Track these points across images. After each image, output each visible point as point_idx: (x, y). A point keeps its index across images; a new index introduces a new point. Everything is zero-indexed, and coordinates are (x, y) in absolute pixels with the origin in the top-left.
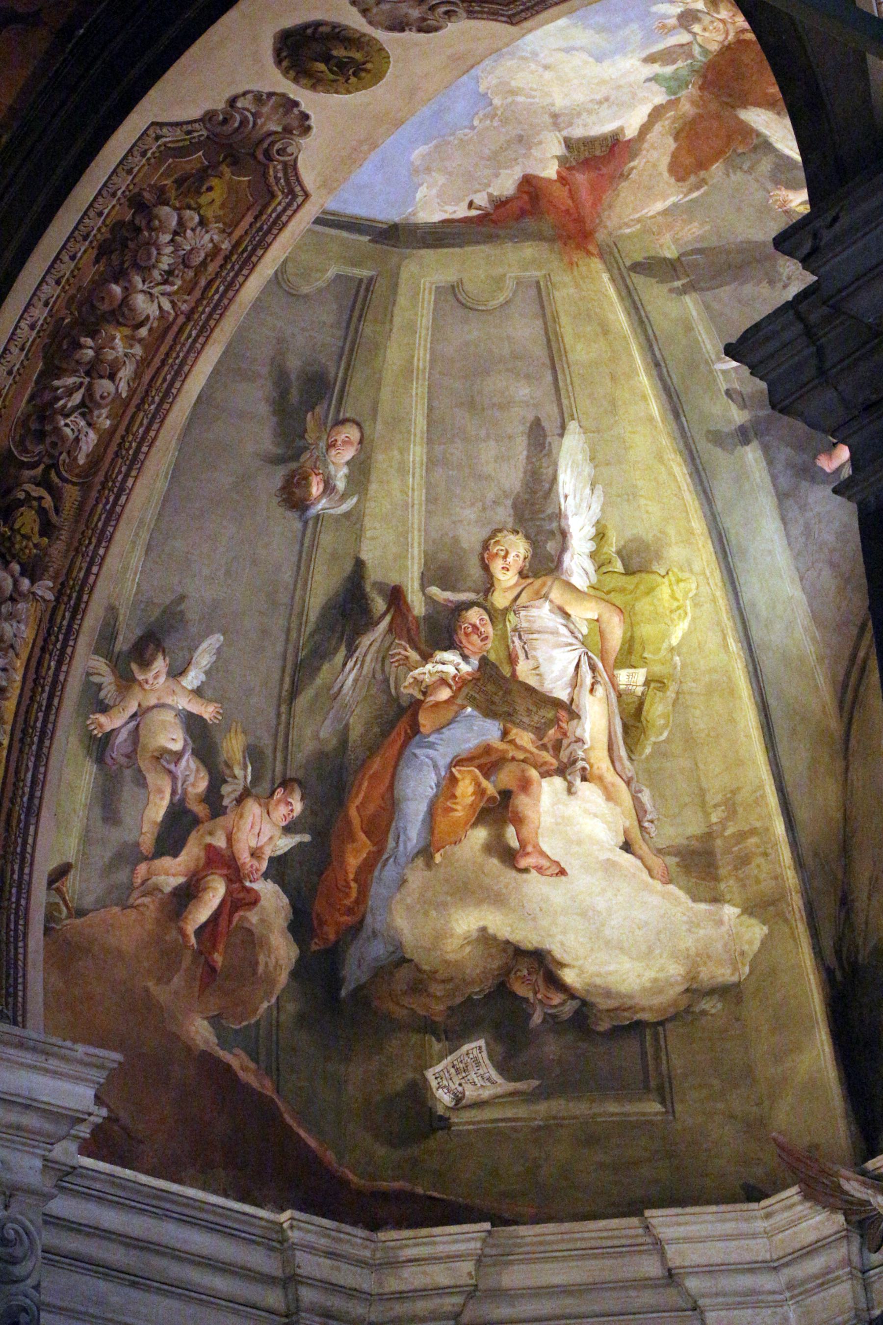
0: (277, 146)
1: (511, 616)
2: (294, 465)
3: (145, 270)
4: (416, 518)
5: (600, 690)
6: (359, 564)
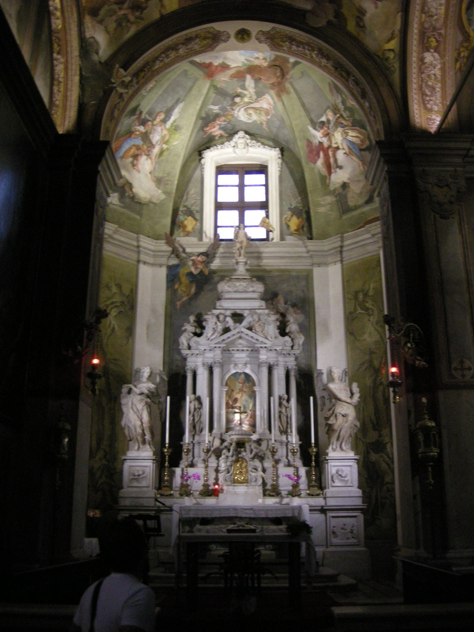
6: (139, 105)
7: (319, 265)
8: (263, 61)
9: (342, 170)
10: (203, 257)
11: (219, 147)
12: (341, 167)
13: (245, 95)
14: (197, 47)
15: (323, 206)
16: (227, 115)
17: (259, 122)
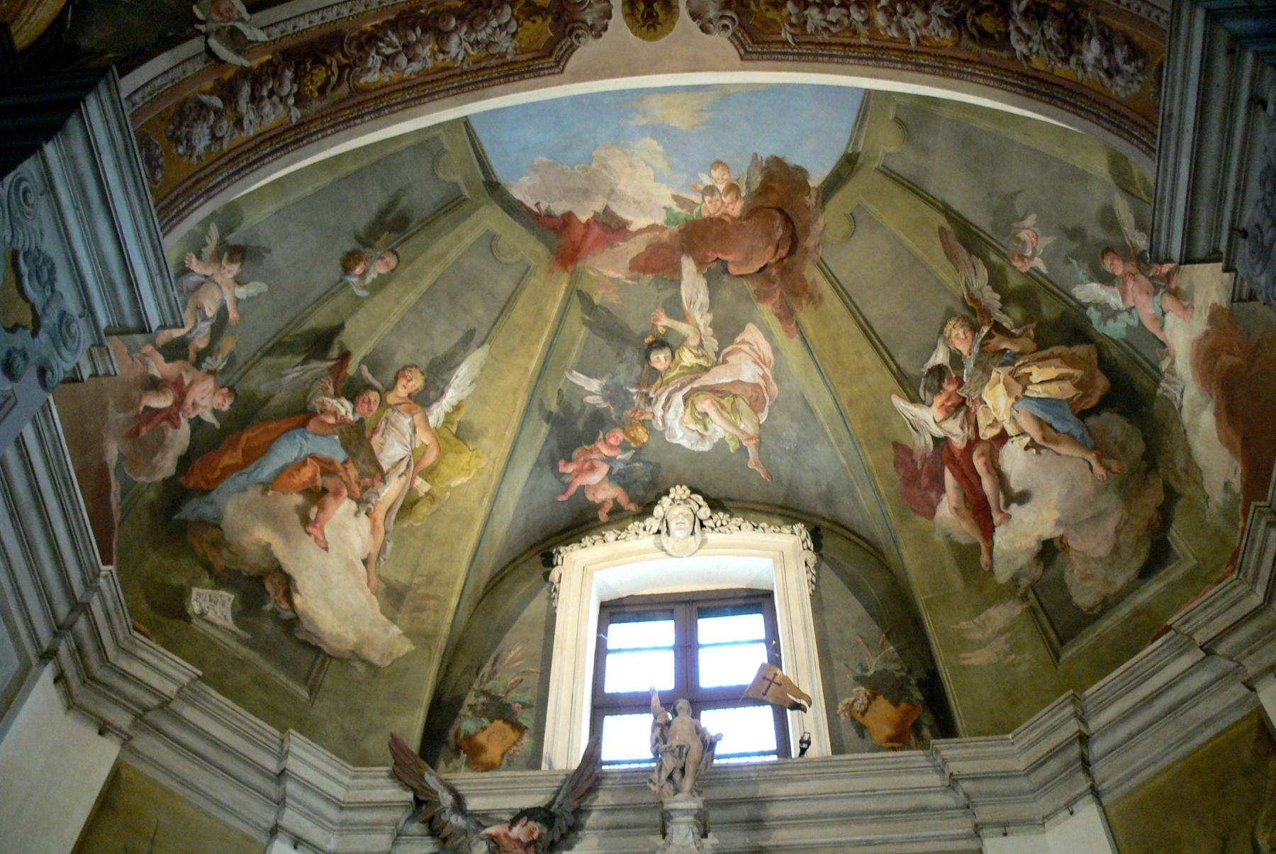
0: (580, 32)
1: (390, 411)
2: (361, 248)
3: (472, 28)
4: (385, 328)
5: (404, 479)
6: (341, 327)
7: (1005, 828)
8: (727, 199)
9: (1028, 506)
10: (531, 824)
11: (610, 535)
12: (1023, 498)
13: (684, 339)
14: (505, 44)
15: (981, 645)
16: (632, 426)
17: (733, 446)
